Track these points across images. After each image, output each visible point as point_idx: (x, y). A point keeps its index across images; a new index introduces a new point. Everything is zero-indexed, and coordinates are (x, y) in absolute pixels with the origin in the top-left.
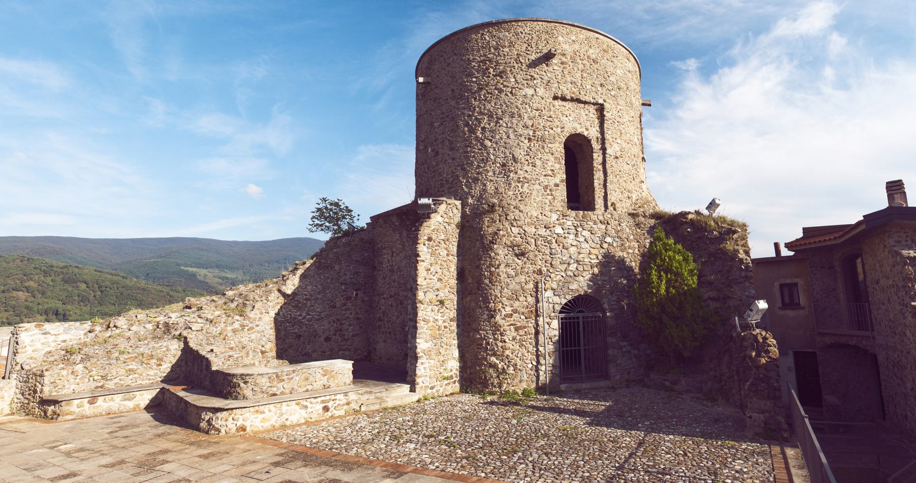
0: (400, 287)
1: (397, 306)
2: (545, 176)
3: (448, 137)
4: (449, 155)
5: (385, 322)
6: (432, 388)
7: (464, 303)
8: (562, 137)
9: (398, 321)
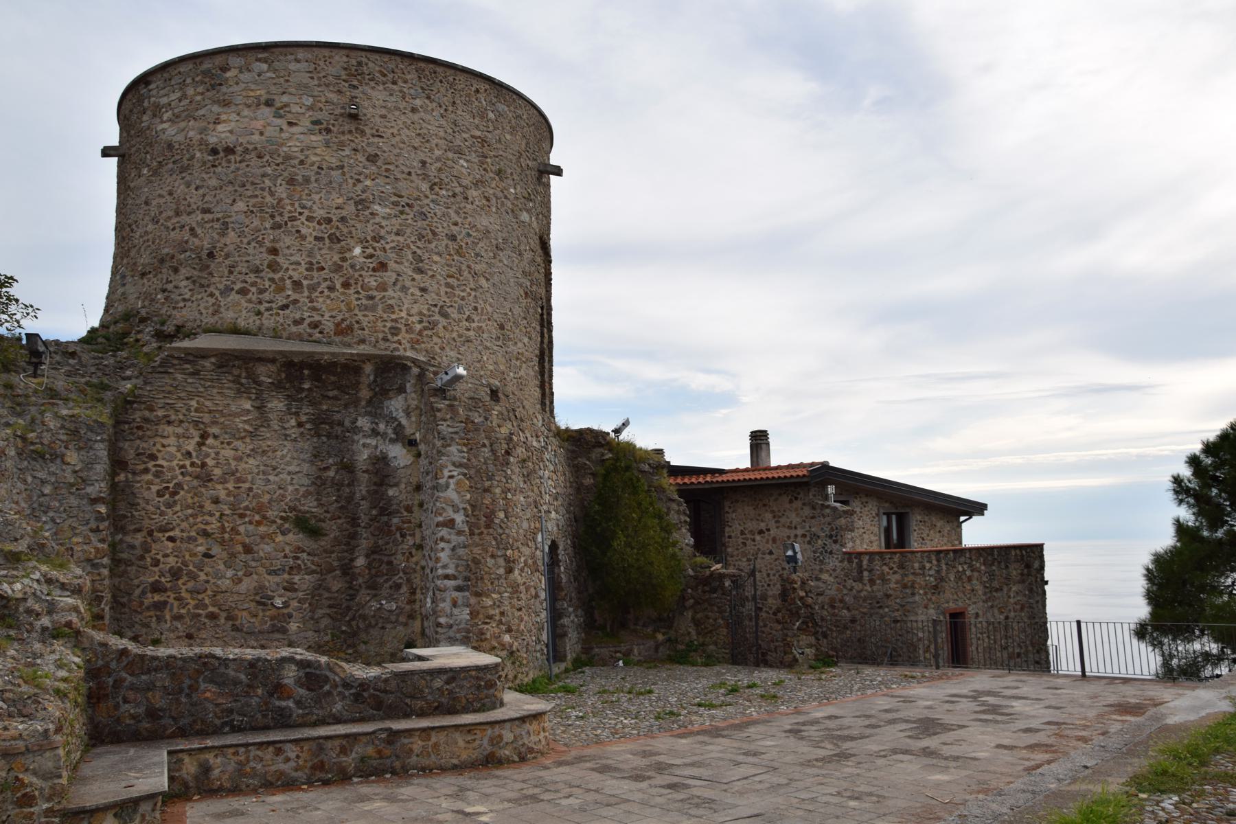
0: (242, 516)
1: (233, 555)
4: (413, 280)
5: (184, 594)
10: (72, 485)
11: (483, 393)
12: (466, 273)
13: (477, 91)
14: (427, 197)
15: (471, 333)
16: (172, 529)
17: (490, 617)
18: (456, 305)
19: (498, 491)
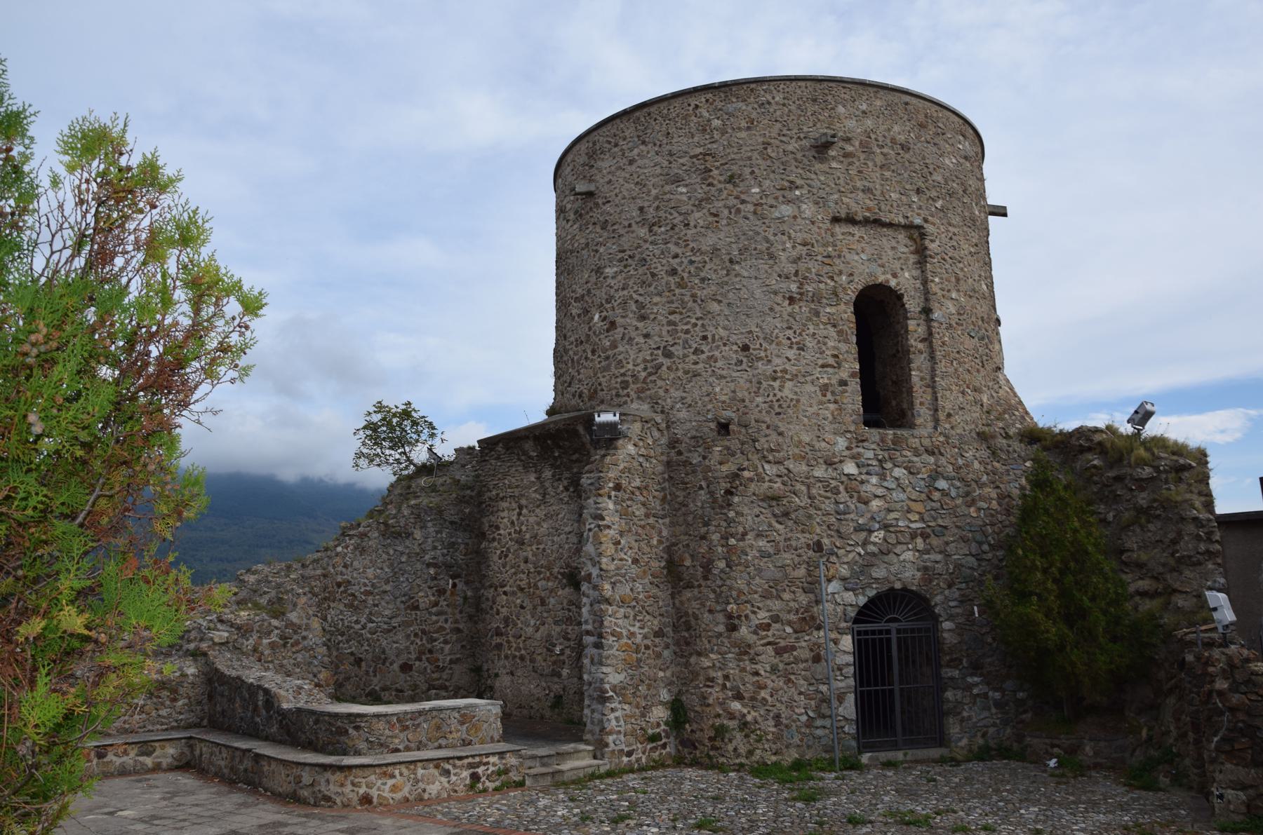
0: (539, 573)
1: (535, 608)
2: (823, 366)
3: (635, 296)
4: (637, 329)
5: (511, 639)
6: (629, 754)
7: (677, 602)
8: (849, 292)
9: (538, 635)
10: (418, 554)
11: (706, 430)
12: (690, 304)
13: (697, 106)
14: (646, 241)
15: (701, 366)
16: (505, 586)
17: (712, 680)
18: (681, 341)
19: (715, 537)
